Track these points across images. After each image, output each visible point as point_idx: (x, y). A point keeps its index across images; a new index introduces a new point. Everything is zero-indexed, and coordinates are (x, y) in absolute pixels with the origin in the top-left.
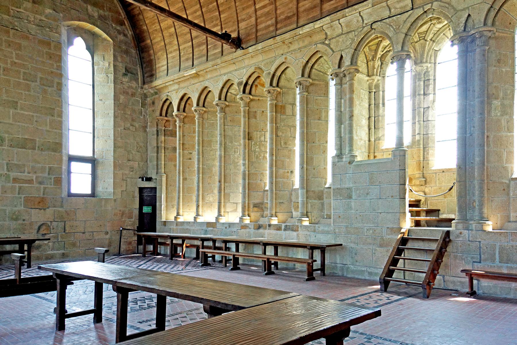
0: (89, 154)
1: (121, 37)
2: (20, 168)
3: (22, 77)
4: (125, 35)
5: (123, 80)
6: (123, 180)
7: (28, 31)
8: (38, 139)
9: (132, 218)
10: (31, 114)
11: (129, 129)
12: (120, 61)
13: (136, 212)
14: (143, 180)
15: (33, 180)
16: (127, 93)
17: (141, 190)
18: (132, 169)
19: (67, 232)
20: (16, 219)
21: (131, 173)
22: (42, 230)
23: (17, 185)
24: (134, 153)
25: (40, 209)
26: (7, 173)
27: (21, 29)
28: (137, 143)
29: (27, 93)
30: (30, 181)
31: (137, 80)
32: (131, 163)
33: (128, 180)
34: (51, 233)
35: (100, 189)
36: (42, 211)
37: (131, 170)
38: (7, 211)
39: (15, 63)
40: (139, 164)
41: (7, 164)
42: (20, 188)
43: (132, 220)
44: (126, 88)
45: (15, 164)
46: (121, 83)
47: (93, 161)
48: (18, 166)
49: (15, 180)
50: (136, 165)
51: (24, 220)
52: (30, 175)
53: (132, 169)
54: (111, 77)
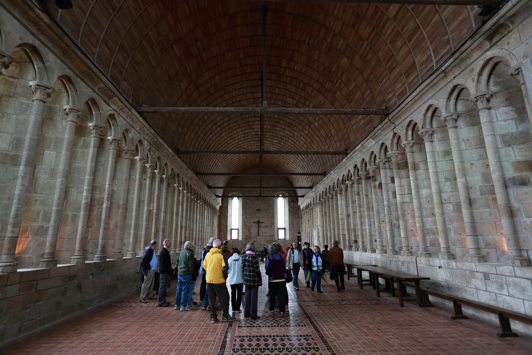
2: (265, 233)
16: (293, 208)
18: (295, 230)
30: (267, 236)
31: (295, 203)
47: (284, 229)
48: (265, 233)
49: (264, 236)
53: (295, 230)
54: (288, 204)
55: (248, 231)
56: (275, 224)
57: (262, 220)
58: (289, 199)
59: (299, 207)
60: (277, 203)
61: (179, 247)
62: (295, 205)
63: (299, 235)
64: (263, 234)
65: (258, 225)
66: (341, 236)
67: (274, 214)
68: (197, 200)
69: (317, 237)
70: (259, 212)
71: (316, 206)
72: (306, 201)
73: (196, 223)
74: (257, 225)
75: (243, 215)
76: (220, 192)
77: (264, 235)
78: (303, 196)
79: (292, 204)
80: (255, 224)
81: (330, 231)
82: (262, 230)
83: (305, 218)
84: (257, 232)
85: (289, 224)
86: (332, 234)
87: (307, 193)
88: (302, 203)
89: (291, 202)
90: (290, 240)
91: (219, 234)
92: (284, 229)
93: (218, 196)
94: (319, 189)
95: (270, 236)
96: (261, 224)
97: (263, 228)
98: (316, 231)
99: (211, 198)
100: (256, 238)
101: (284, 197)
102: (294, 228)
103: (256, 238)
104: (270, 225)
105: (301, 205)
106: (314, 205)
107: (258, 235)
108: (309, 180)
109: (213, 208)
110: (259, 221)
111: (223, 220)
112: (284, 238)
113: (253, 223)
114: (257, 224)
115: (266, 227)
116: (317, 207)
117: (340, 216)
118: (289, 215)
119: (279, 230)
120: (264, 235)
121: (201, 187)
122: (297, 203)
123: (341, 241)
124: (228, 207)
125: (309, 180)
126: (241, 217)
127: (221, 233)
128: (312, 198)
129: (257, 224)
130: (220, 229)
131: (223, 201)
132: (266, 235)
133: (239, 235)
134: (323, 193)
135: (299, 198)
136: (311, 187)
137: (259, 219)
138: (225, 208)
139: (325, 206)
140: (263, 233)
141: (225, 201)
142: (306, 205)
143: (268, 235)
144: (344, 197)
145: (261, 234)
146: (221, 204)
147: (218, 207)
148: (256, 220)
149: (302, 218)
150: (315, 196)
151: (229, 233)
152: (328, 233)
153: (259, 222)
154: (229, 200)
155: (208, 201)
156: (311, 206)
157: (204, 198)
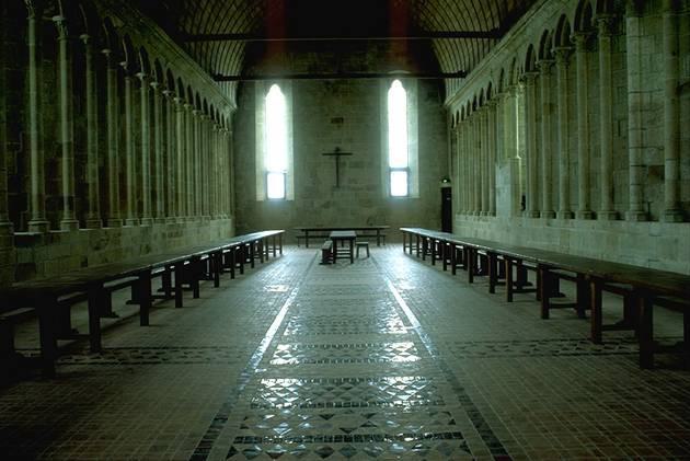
0: (405, 166)
49: (354, 189)
57: (346, 148)
59: (444, 114)
60: (385, 102)
61: (40, 216)
62: (435, 105)
63: (445, 184)
65: (337, 159)
66: (632, 172)
68: (134, 68)
69: (509, 186)
71: (509, 94)
72: (475, 84)
73: (139, 144)
74: (334, 161)
76: (230, 66)
77: (353, 185)
78: (461, 75)
81: (569, 164)
82: (348, 173)
83: (465, 138)
86: (580, 171)
87: (476, 60)
88: (458, 97)
89: (426, 100)
91: (235, 185)
92: (407, 170)
93: (219, 78)
94: (529, 31)
98: (508, 167)
99: (198, 81)
101: (405, 79)
105: (454, 105)
106: (500, 91)
107: (338, 186)
108: (488, 14)
109: (212, 115)
110: (338, 149)
113: (324, 154)
115: (357, 165)
116: (514, 96)
117: (630, 96)
121: (142, 28)
122: (443, 101)
123: (632, 188)
125: (488, 14)
128: (497, 74)
134: (542, 42)
135: (449, 82)
136: (496, 35)
137: (339, 146)
139: (551, 85)
142: (471, 101)
144: (666, 16)
145: (344, 183)
146: (235, 106)
147: (226, 113)
148: (331, 148)
149: (454, 141)
150: (510, 61)
151: (259, 180)
152: (561, 167)
153: (338, 153)
154: (257, 96)
155: (186, 84)
156: (488, 98)
157: (165, 71)
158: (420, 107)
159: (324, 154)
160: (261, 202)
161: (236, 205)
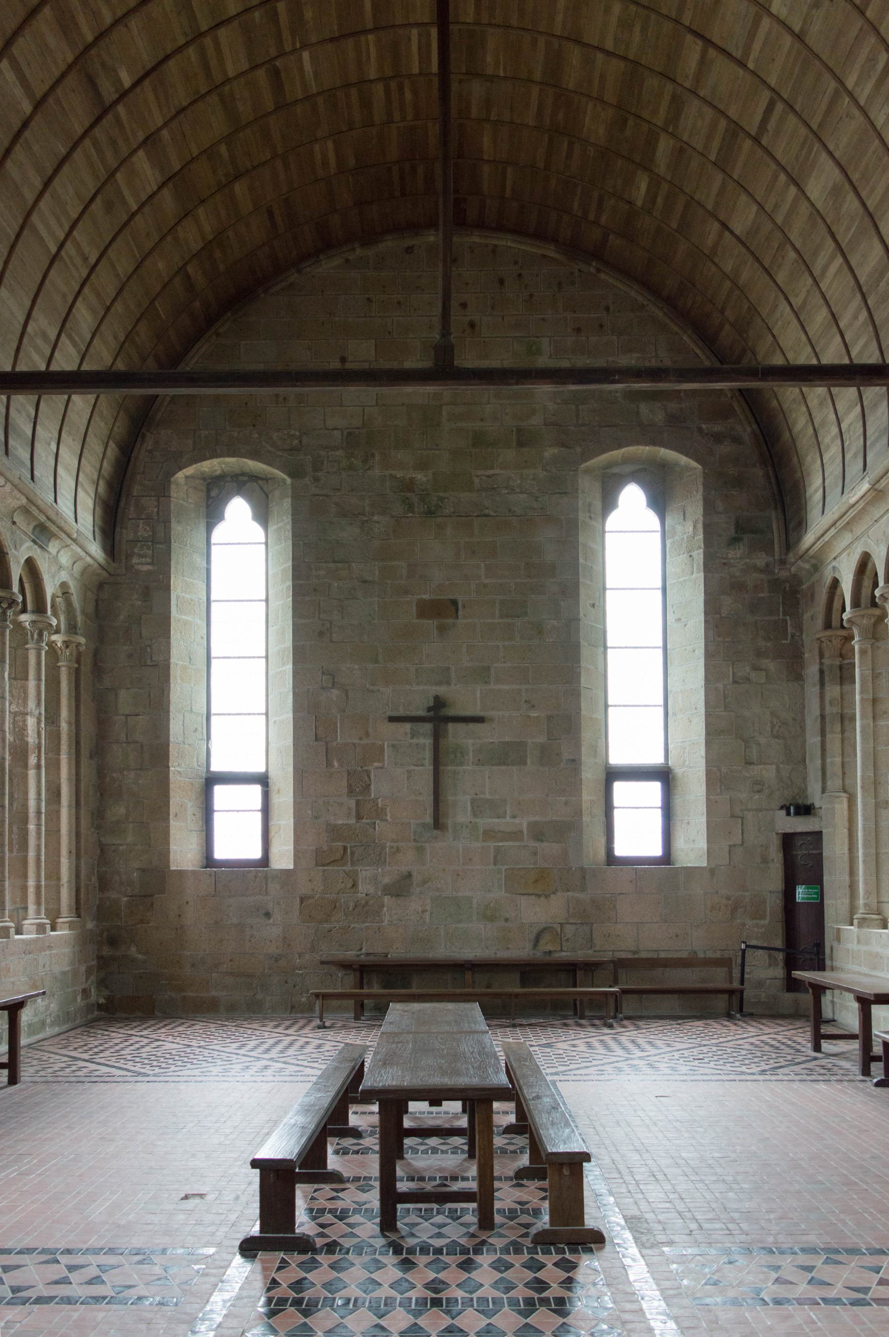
1: (725, 448)
3: (497, 612)
4: (736, 440)
5: (730, 556)
6: (732, 816)
7: (510, 511)
8: (530, 741)
9: (763, 917)
10: (518, 687)
11: (748, 680)
12: (721, 509)
13: (774, 902)
14: (788, 814)
15: (521, 832)
17: (788, 841)
18: (758, 786)
19: (597, 949)
20: (492, 918)
21: (757, 796)
22: (542, 942)
23: (492, 844)
24: (762, 740)
25: (538, 896)
26: (473, 820)
27: (495, 512)
28: (772, 713)
29: (507, 643)
30: (516, 835)
31: (768, 548)
32: (756, 770)
33: (749, 815)
34: (561, 950)
35: (680, 844)
36: (543, 899)
37: (757, 788)
38: (475, 901)
39: (485, 586)
40: (778, 770)
41: (473, 801)
42: (498, 850)
43: (762, 922)
44: (738, 574)
45: (488, 800)
46: (725, 564)
49: (489, 834)
50: (769, 773)
51: (506, 920)
52: (517, 821)
53: (758, 786)
54: (699, 555)
55: (351, 791)
56: (586, 735)
58: (709, 507)
62: (761, 560)
64: (477, 811)
65: (437, 736)
67: (577, 646)
70: (442, 629)
74: (428, 742)
75: (299, 654)
77: (486, 822)
79: (736, 553)
80: (408, 726)
84: (427, 798)
85: (712, 733)
89: (734, 541)
90: (712, 871)
91: (99, 815)
95: (538, 833)
96: (456, 733)
97: (479, 762)
100: (420, 850)
102: (749, 763)
103: (420, 850)
104: (542, 739)
107: (438, 824)
110: (439, 703)
111: (125, 700)
112: (655, 850)
113: (392, 719)
114: (428, 727)
118: (709, 656)
119: (619, 787)
120: (486, 822)
124: (166, 588)
126: (289, 667)
127: (118, 811)
129: (428, 727)
130: (101, 772)
131: (126, 534)
132: (506, 823)
133: (273, 823)
137: (441, 690)
138: (146, 594)
140: (478, 807)
141: (143, 531)
143: (523, 823)
154: (176, 528)
158: (710, 565)
159: (392, 719)
160: (181, 873)
161: (104, 884)
